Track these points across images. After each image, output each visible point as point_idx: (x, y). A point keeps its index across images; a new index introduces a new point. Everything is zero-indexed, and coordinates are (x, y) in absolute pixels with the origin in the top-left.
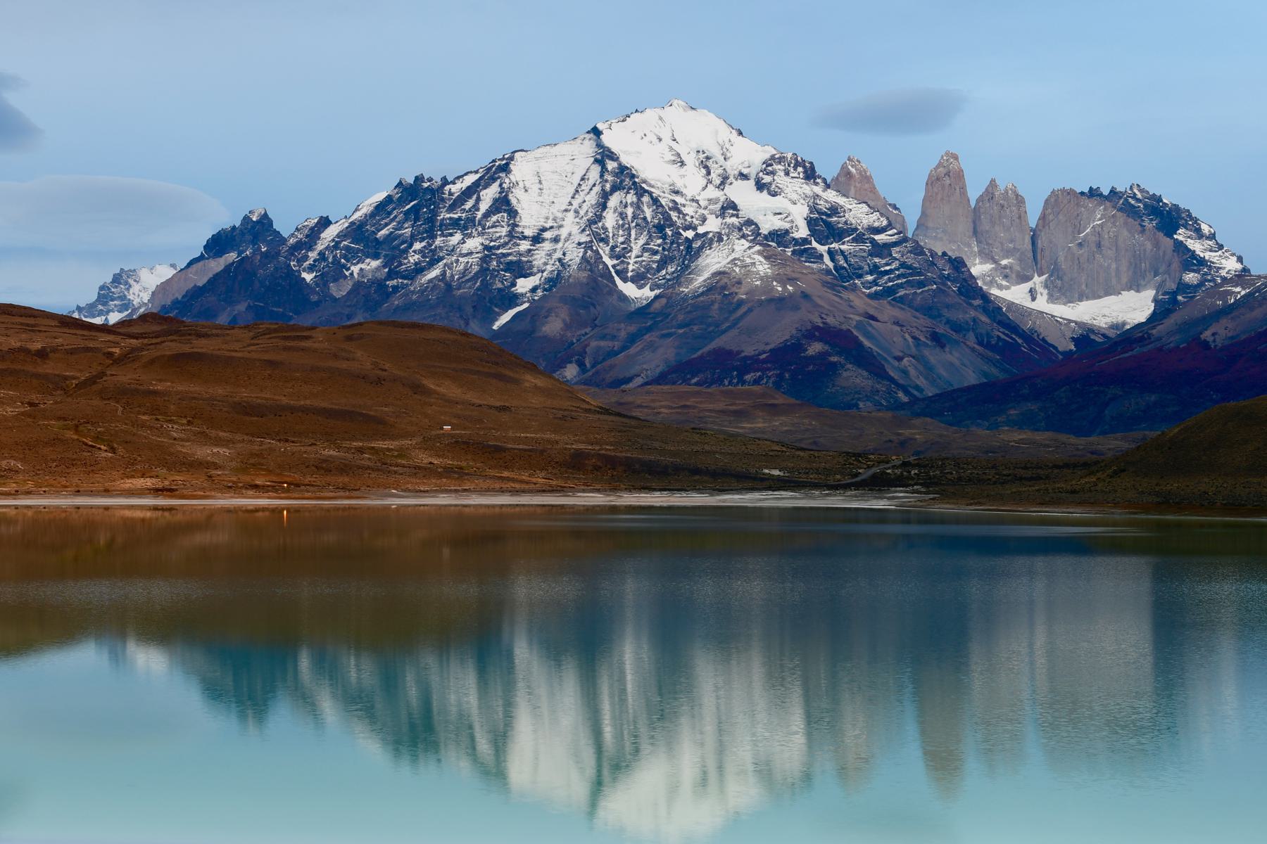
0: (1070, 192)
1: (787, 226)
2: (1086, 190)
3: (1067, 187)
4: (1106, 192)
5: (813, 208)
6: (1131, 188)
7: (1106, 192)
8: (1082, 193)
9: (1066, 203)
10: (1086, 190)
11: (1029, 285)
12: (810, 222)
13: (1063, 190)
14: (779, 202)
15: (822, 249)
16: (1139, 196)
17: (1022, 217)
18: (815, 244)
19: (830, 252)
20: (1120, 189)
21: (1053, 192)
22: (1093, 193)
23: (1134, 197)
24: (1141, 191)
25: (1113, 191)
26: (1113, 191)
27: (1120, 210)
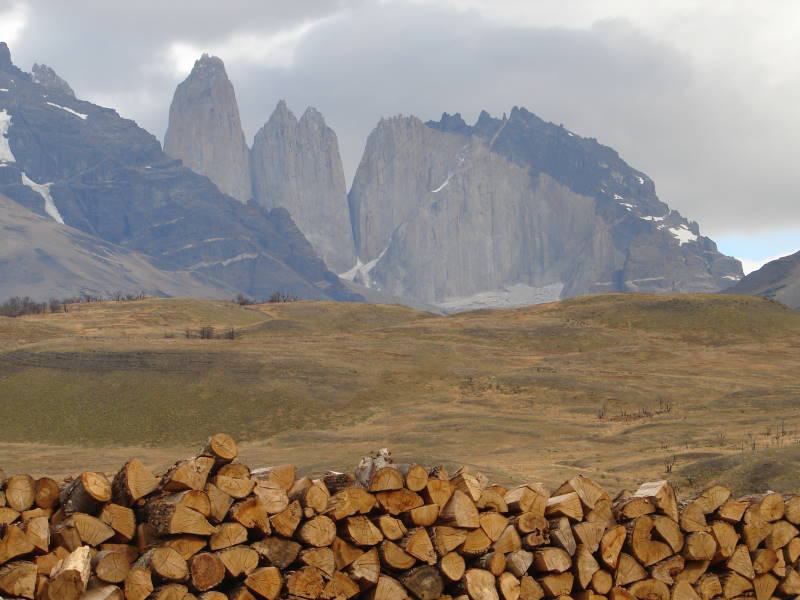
0: (411, 122)
2: (438, 119)
3: (406, 115)
4: (471, 120)
7: (471, 120)
8: (431, 124)
10: (438, 119)
13: (397, 120)
15: (42, 189)
18: (26, 181)
19: (53, 192)
21: (382, 122)
22: (451, 124)
25: (484, 116)
26: (484, 116)
27: (495, 148)
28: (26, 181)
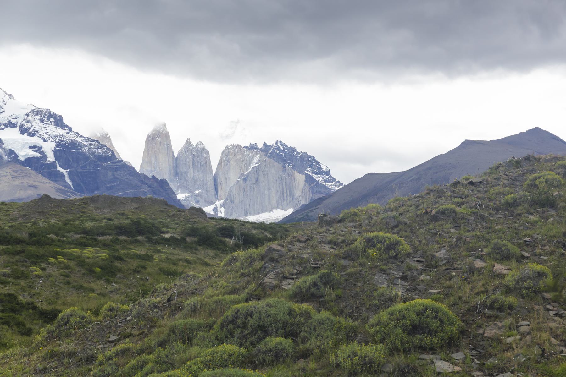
1: (39, 155)
2: (248, 145)
4: (260, 146)
5: (58, 145)
6: (276, 143)
8: (246, 147)
9: (232, 153)
11: (213, 206)
12: (55, 152)
14: (35, 140)
16: (281, 148)
17: (207, 162)
18: (59, 168)
19: (70, 174)
20: (269, 143)
22: (253, 147)
23: (278, 148)
24: (284, 145)
27: (269, 157)
28: (59, 168)
